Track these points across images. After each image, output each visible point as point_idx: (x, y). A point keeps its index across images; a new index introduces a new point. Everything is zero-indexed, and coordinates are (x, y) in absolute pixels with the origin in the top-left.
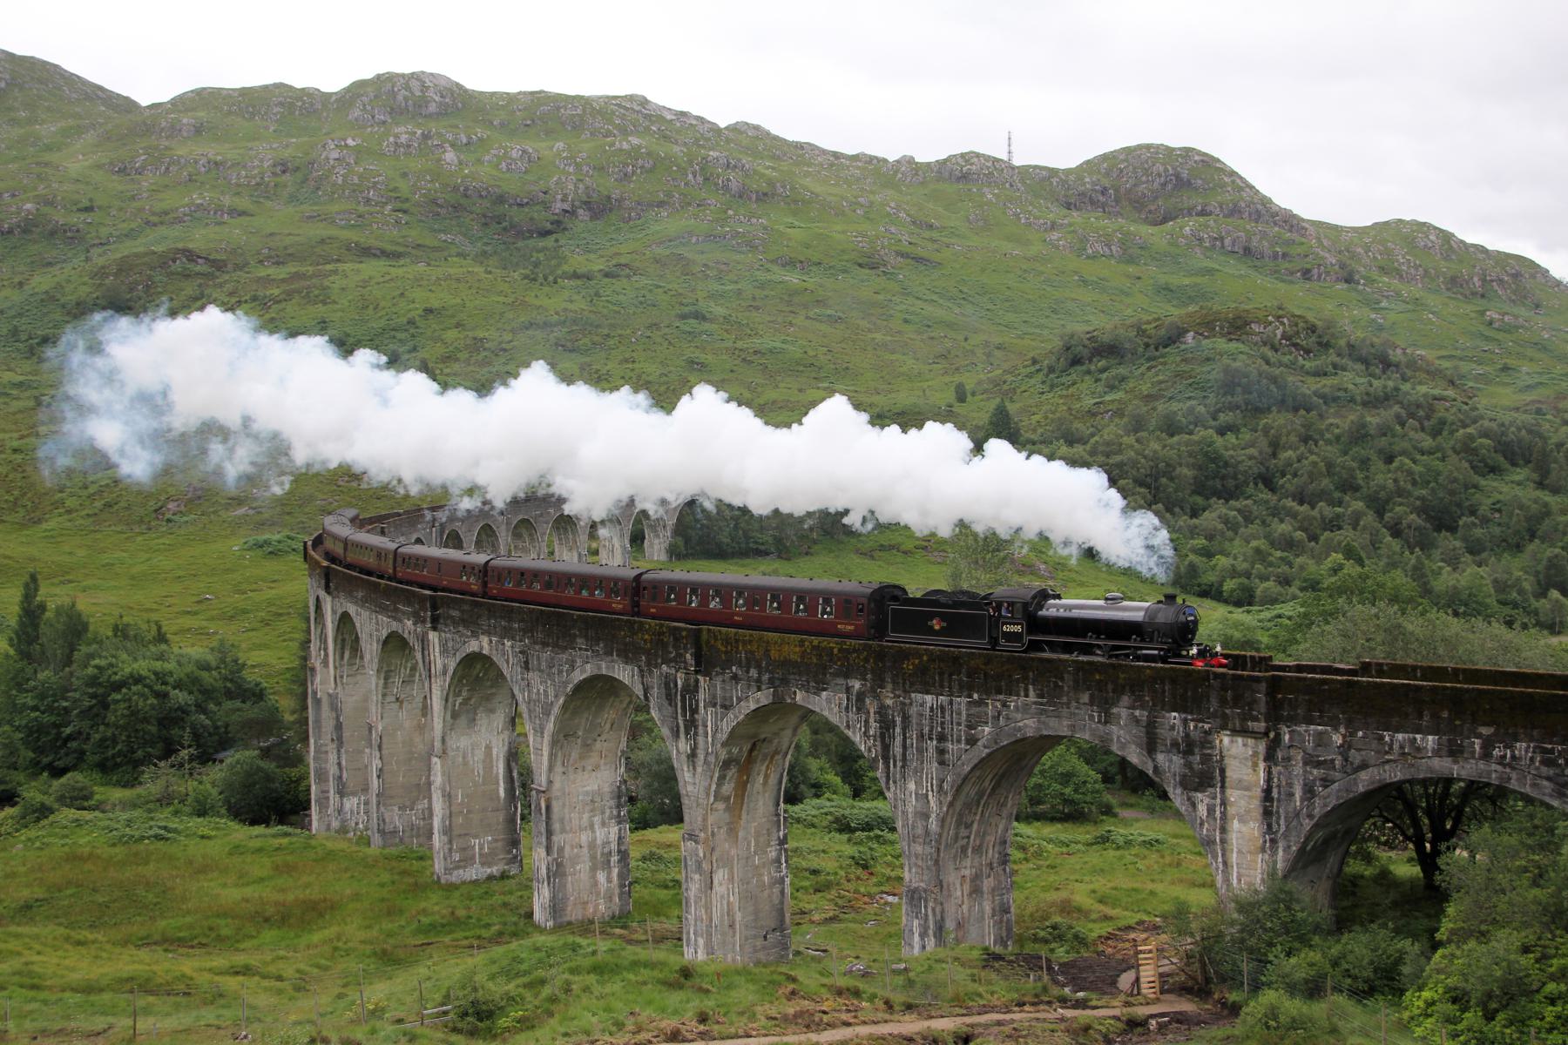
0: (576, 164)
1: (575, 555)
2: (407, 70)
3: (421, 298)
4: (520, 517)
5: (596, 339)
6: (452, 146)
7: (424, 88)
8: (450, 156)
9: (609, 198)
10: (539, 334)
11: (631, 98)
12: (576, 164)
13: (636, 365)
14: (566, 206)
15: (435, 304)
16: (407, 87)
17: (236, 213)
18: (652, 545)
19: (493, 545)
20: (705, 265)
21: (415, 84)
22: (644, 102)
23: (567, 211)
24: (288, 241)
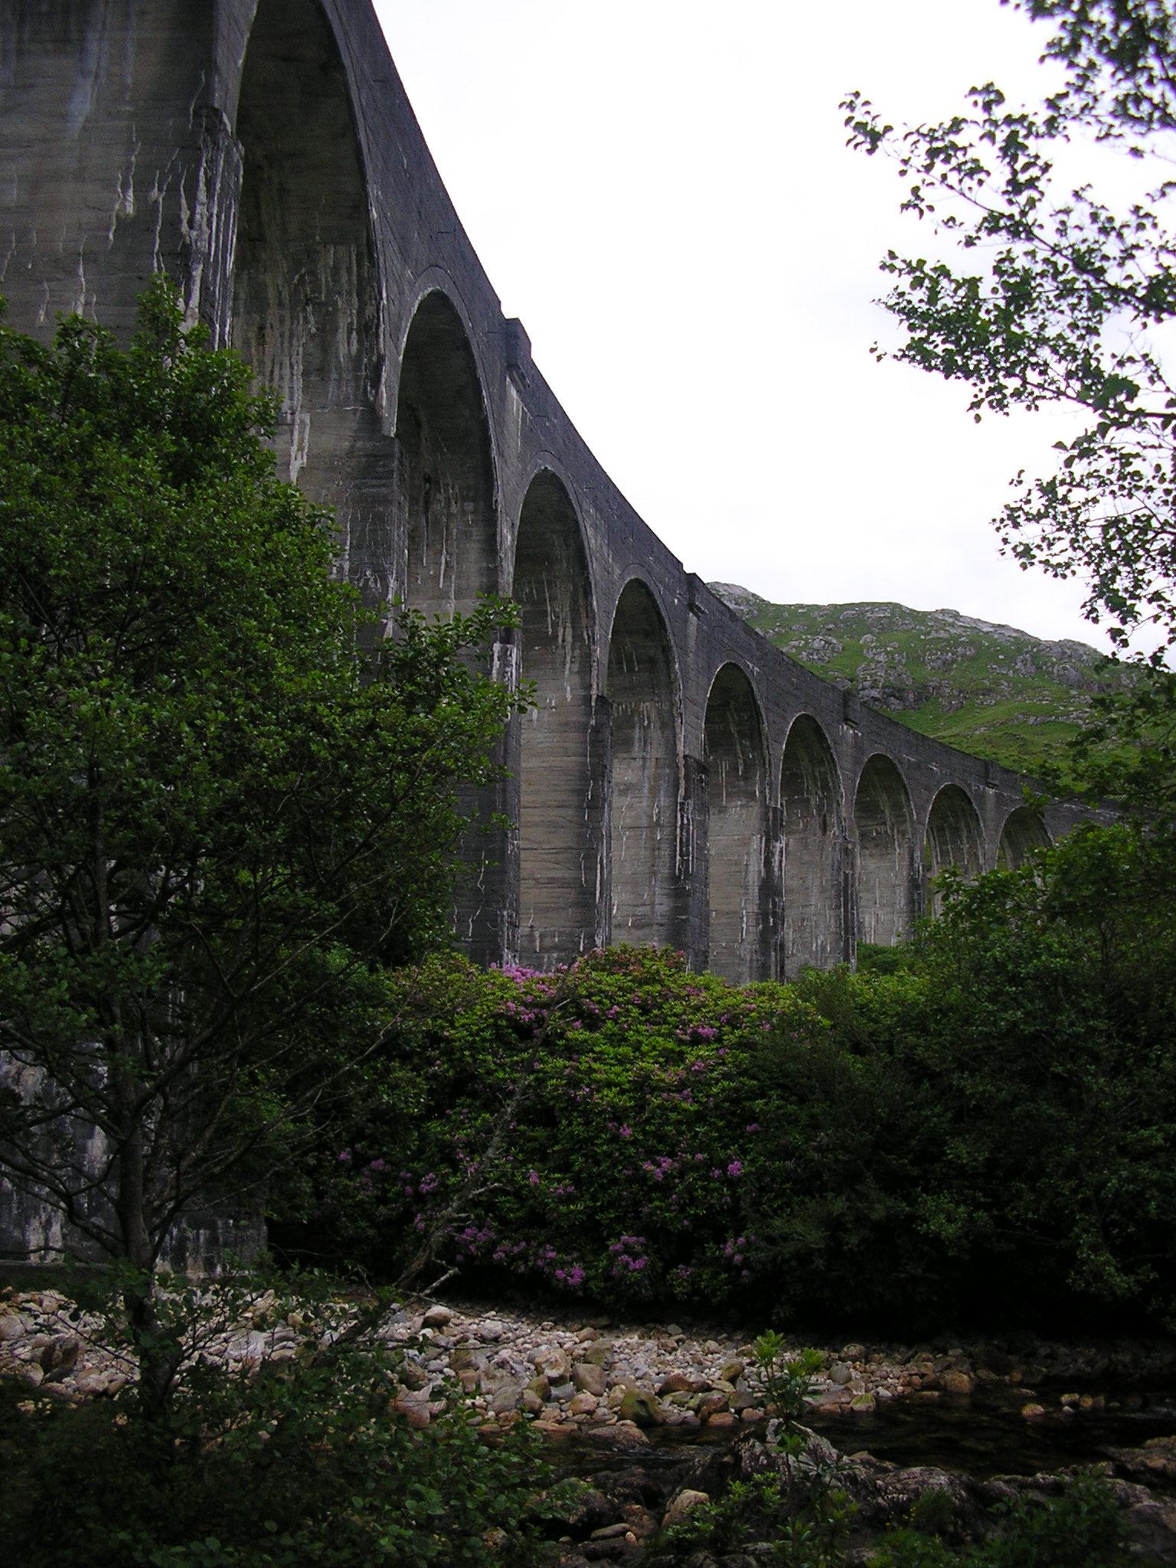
0: (887, 653)
4: (879, 750)
9: (926, 687)
11: (943, 611)
12: (887, 653)
14: (875, 693)
19: (825, 787)
22: (956, 615)
23: (875, 699)
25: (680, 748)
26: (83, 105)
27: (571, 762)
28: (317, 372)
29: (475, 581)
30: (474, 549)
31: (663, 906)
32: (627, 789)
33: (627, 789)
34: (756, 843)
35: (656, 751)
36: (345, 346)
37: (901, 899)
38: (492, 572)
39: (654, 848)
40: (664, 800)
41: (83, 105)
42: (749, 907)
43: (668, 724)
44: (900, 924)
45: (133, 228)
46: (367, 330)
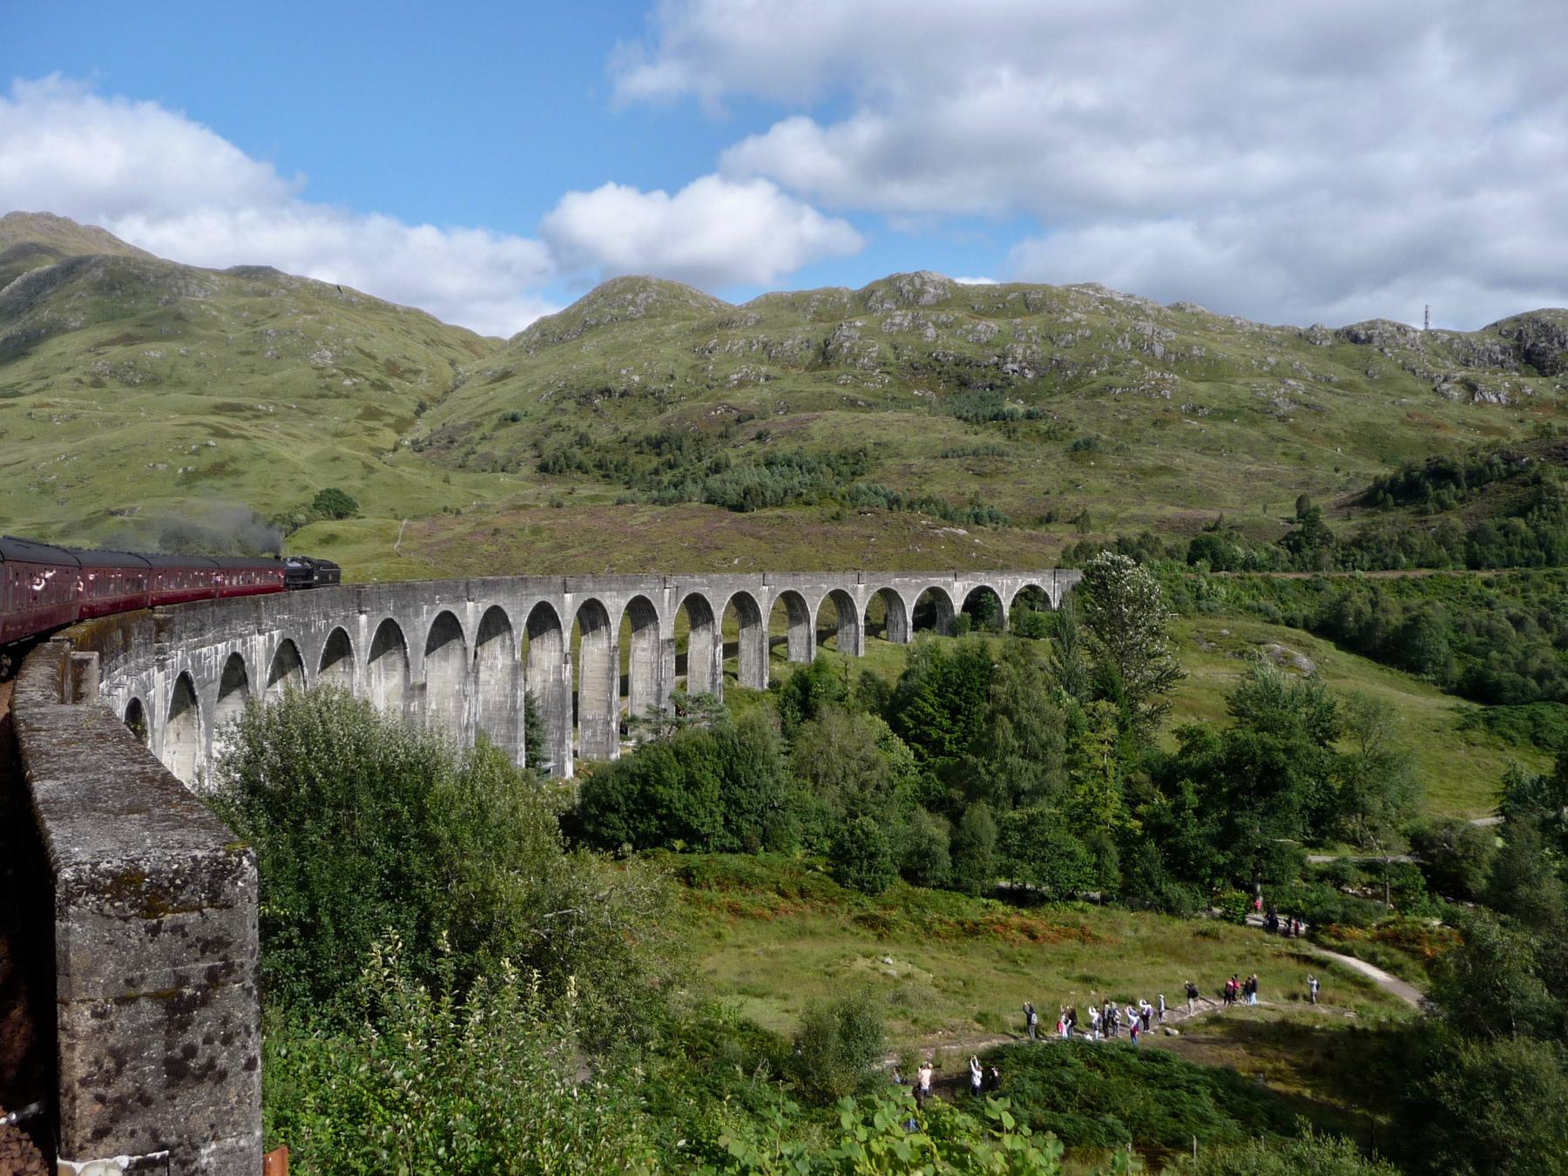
1: (853, 625)
2: (910, 270)
3: (873, 434)
5: (1000, 465)
6: (934, 323)
7: (924, 283)
8: (931, 332)
10: (956, 461)
13: (1027, 486)
14: (1015, 367)
15: (885, 439)
16: (912, 282)
17: (767, 378)
18: (941, 624)
20: (1118, 411)
21: (917, 282)
23: (1014, 371)
24: (798, 395)
25: (662, 637)
26: (449, 671)
27: (606, 665)
28: (503, 647)
29: (558, 648)
30: (557, 640)
31: (655, 688)
32: (644, 650)
33: (644, 650)
34: (711, 647)
35: (653, 638)
36: (508, 642)
37: (805, 641)
38: (562, 645)
39: (652, 670)
40: (655, 654)
41: (449, 671)
42: (708, 670)
43: (657, 629)
44: (804, 652)
45: (458, 691)
46: (512, 640)
